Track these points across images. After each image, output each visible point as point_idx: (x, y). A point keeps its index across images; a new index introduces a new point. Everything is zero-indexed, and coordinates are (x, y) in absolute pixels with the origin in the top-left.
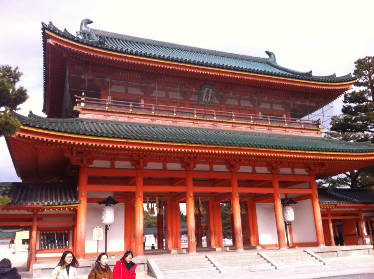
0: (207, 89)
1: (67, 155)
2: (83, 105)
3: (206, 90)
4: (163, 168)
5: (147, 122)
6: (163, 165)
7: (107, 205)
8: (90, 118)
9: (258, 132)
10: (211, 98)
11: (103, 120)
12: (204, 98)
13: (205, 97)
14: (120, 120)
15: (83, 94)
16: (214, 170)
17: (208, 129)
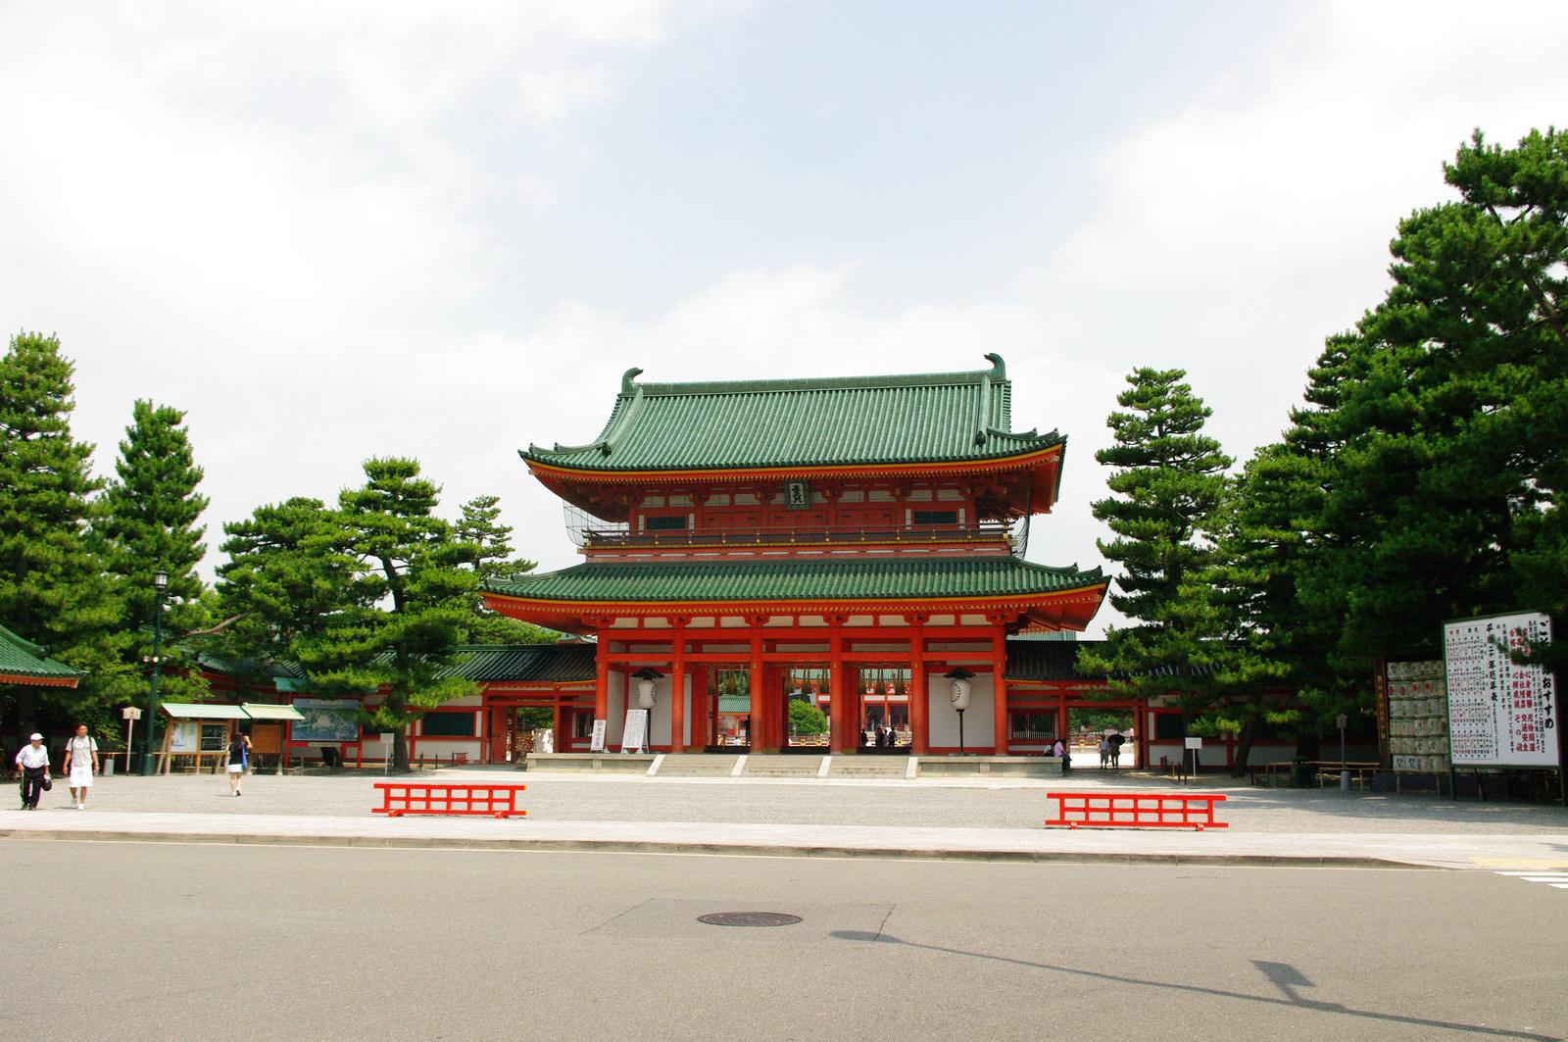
3: (792, 486)
12: (793, 499)
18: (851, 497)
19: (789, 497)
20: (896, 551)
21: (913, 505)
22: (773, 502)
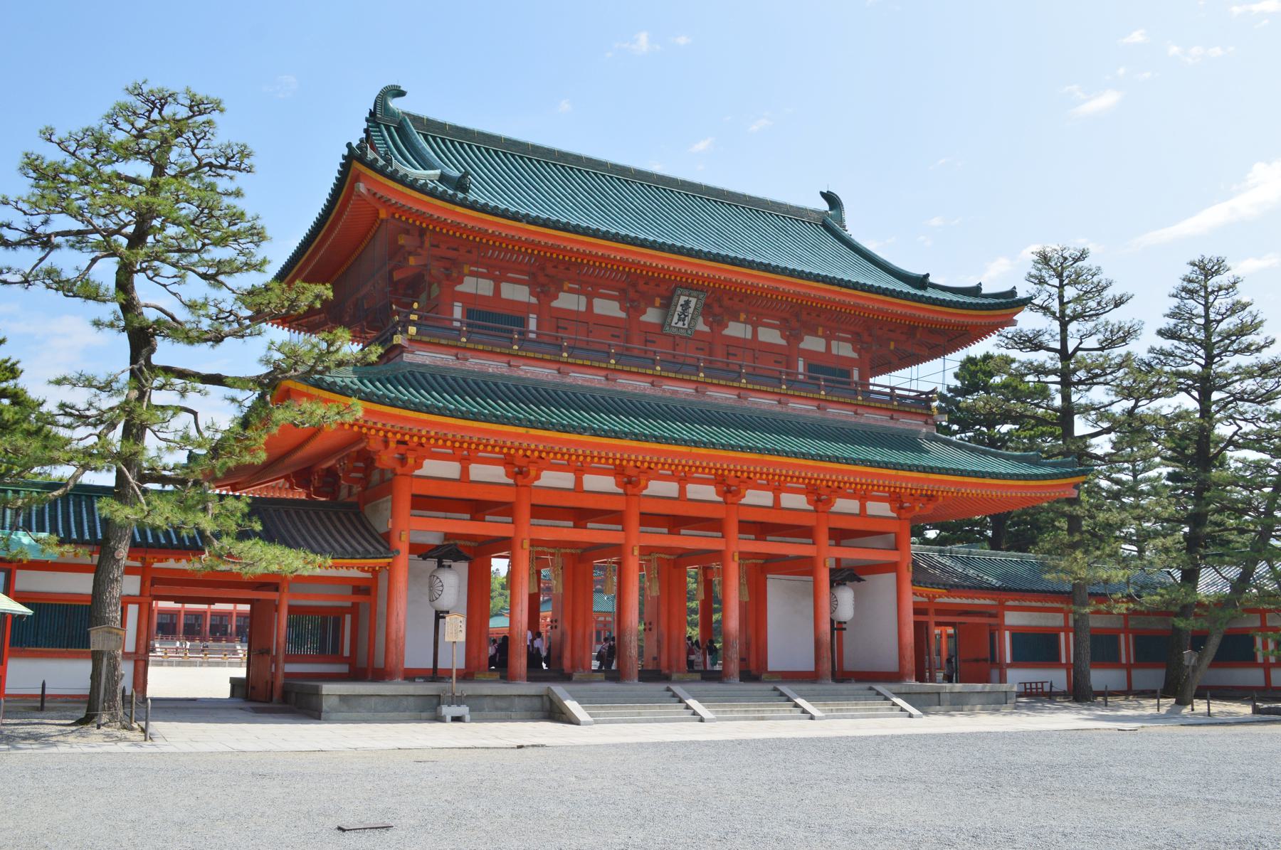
0: (686, 298)
1: (374, 445)
2: (412, 330)
3: (683, 299)
4: (575, 485)
5: (549, 377)
6: (576, 477)
7: (440, 565)
8: (427, 362)
9: (796, 413)
10: (692, 318)
11: (454, 369)
13: (680, 316)
14: (490, 370)
15: (416, 306)
16: (689, 496)
21: (808, 354)
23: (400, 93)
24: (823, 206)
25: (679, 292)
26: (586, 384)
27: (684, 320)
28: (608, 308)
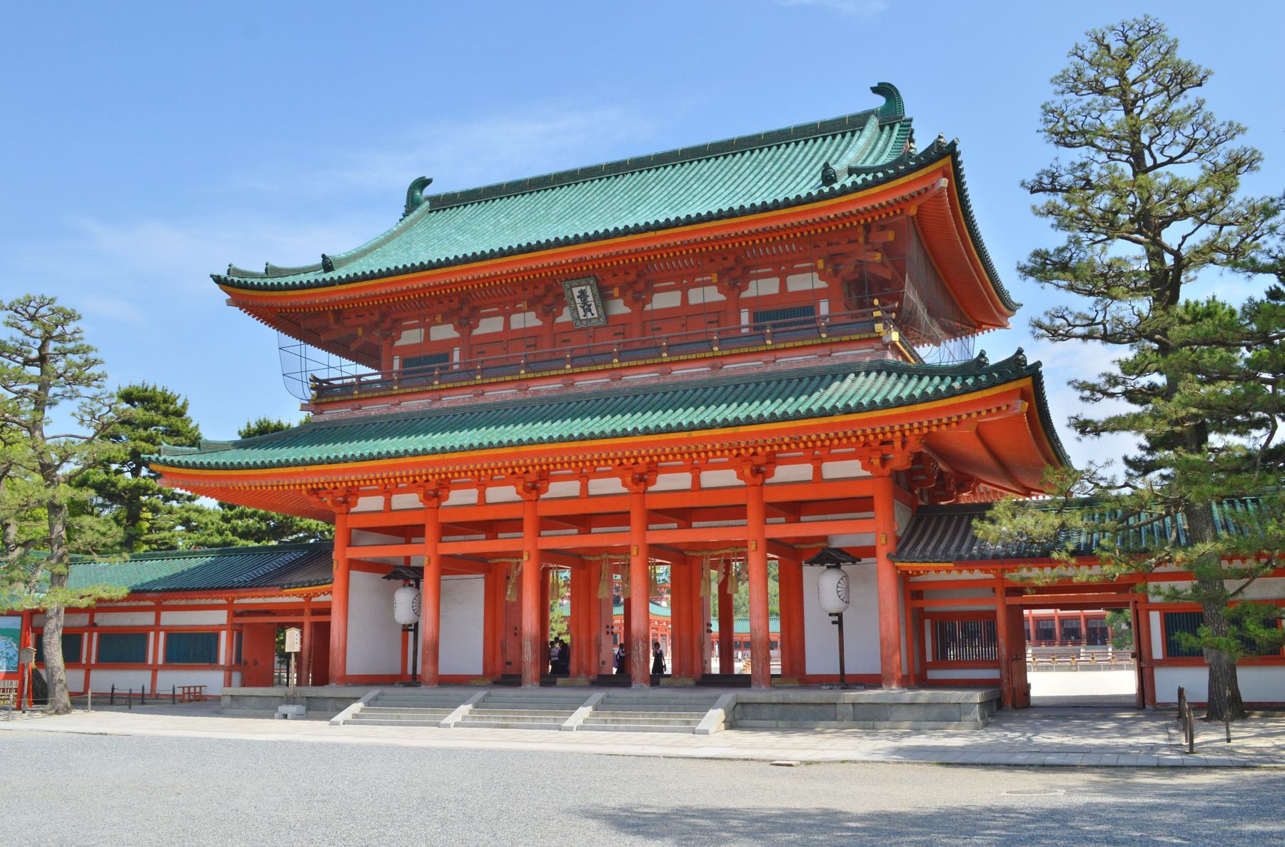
0: (579, 289)
3: (576, 291)
17: (546, 398)
18: (665, 300)
19: (576, 309)
20: (713, 367)
22: (559, 320)
23: (423, 183)
24: (879, 102)
25: (568, 286)
26: (451, 405)
27: (590, 311)
28: (526, 320)
